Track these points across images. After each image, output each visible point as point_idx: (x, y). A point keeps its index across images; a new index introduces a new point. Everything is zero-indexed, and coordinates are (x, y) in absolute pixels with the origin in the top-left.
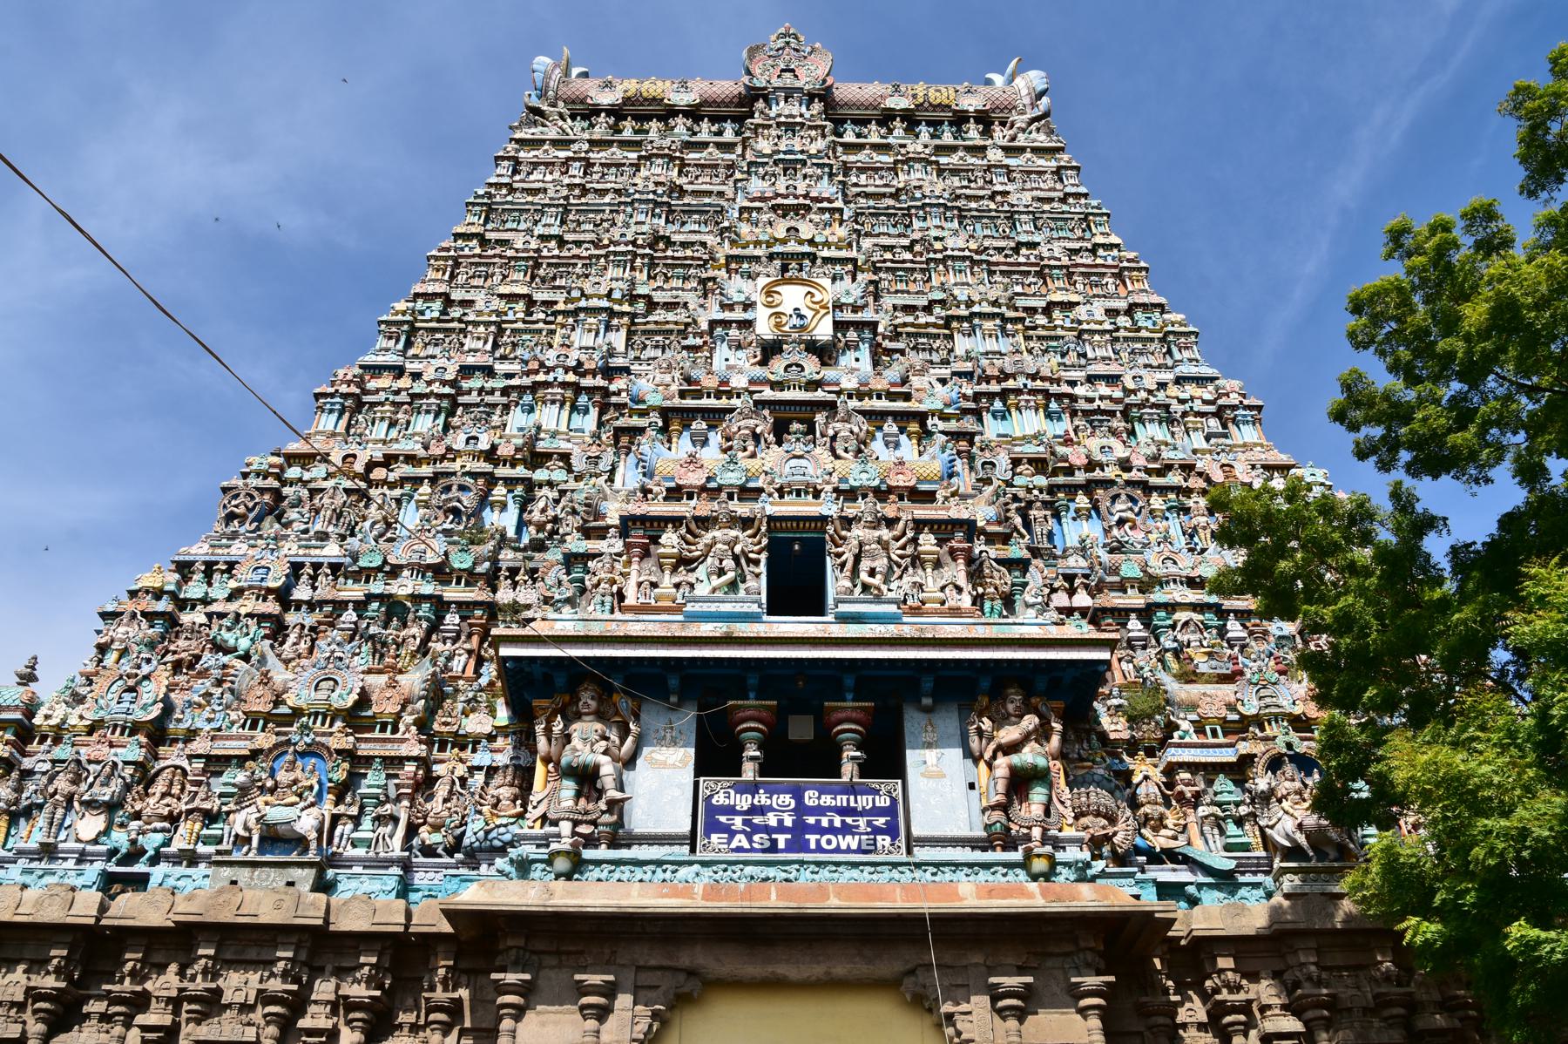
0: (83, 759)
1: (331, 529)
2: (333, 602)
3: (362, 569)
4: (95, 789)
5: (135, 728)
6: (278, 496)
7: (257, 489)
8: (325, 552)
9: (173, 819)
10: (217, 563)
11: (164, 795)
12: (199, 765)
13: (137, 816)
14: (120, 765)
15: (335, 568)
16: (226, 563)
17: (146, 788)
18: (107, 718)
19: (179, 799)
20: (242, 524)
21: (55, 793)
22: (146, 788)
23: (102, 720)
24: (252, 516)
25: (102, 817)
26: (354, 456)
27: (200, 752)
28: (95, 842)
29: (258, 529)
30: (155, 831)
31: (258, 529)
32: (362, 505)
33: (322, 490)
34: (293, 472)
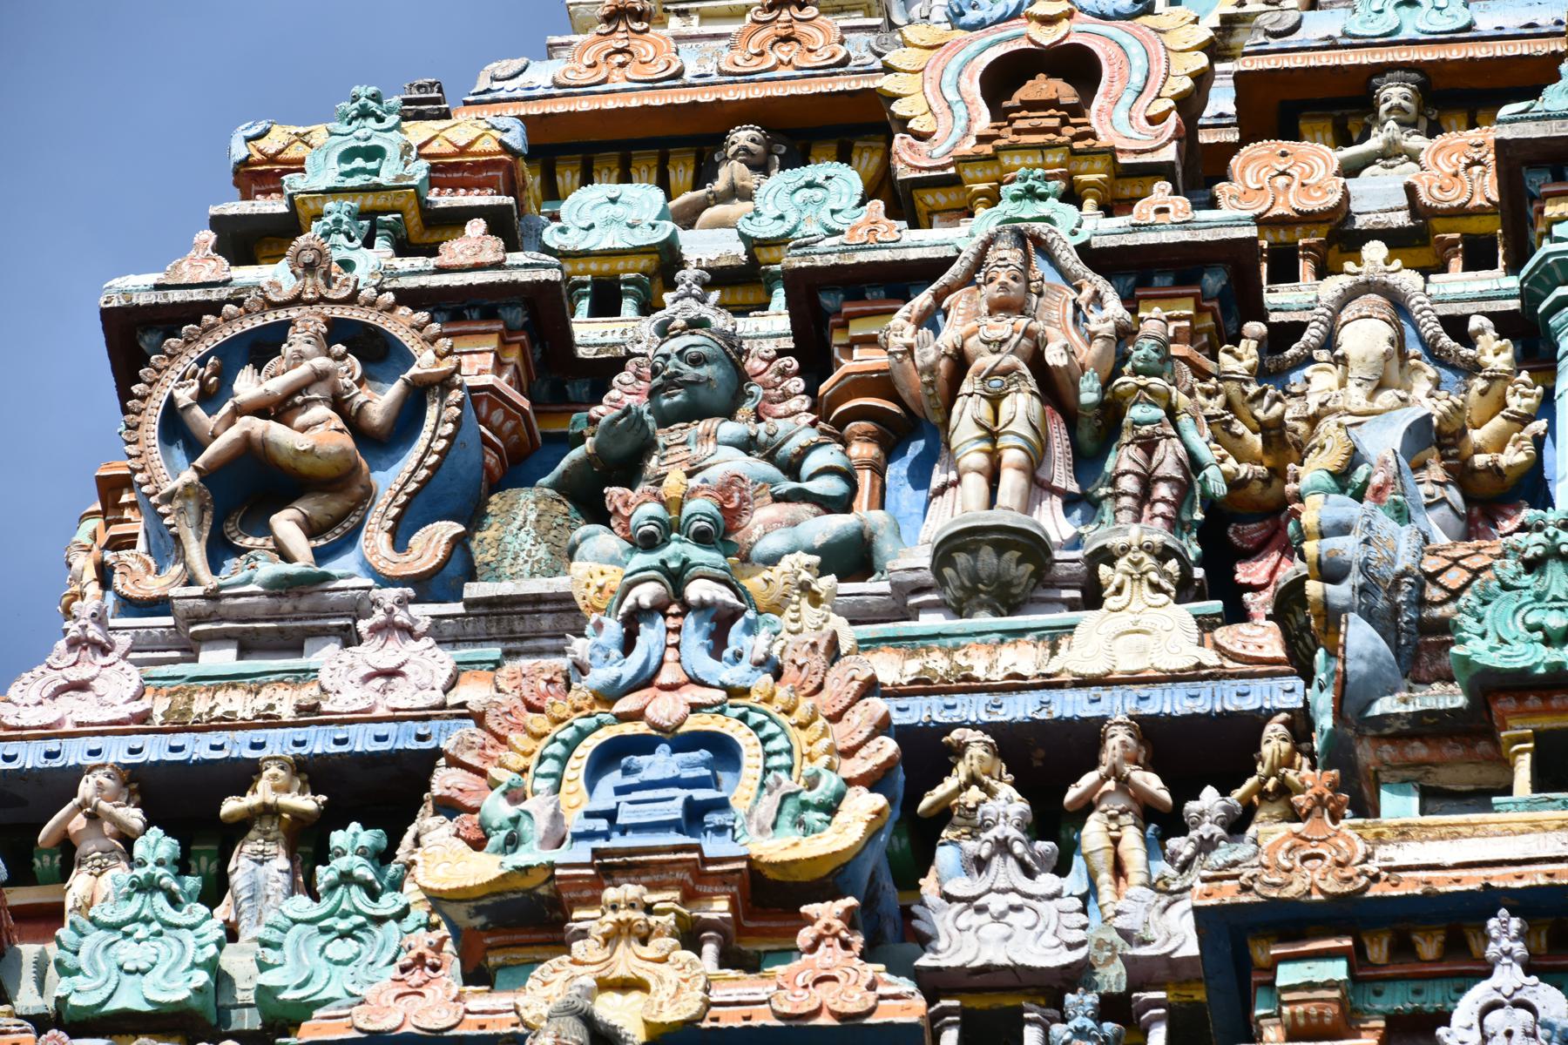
1: (1053, 522)
2: (1346, 916)
3: (1494, 687)
6: (563, 377)
7: (407, 298)
8: (1079, 657)
10: (243, 775)
15: (1201, 752)
16: (310, 771)
20: (334, 534)
24: (392, 481)
26: (1079, 67)
29: (460, 565)
31: (460, 565)
32: (1241, 359)
33: (901, 280)
34: (608, 215)
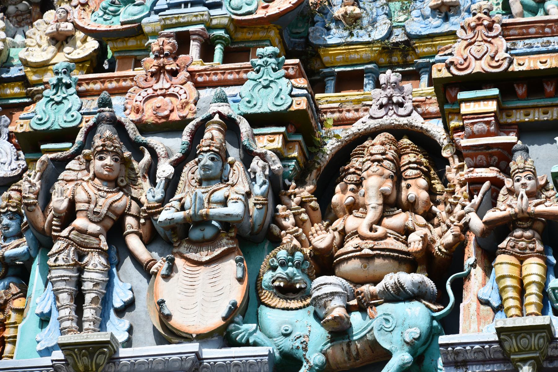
0: (128, 118)
4: (189, 193)
5: (239, 42)
9: (443, 269)
11: (391, 204)
12: (479, 105)
13: (324, 262)
14: (244, 126)
17: (324, 193)
18: (151, 23)
19: (429, 216)
21: (70, 214)
22: (324, 193)
23: (135, 31)
25: (230, 268)
27: (476, 67)
28: (224, 336)
30: (399, 295)
